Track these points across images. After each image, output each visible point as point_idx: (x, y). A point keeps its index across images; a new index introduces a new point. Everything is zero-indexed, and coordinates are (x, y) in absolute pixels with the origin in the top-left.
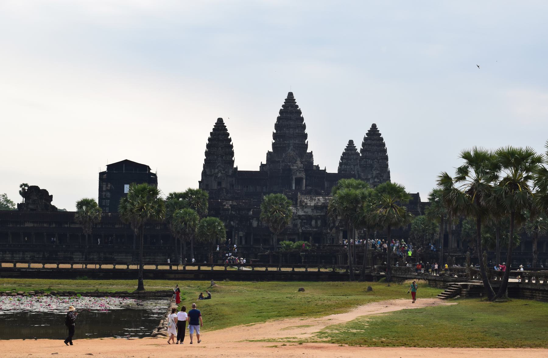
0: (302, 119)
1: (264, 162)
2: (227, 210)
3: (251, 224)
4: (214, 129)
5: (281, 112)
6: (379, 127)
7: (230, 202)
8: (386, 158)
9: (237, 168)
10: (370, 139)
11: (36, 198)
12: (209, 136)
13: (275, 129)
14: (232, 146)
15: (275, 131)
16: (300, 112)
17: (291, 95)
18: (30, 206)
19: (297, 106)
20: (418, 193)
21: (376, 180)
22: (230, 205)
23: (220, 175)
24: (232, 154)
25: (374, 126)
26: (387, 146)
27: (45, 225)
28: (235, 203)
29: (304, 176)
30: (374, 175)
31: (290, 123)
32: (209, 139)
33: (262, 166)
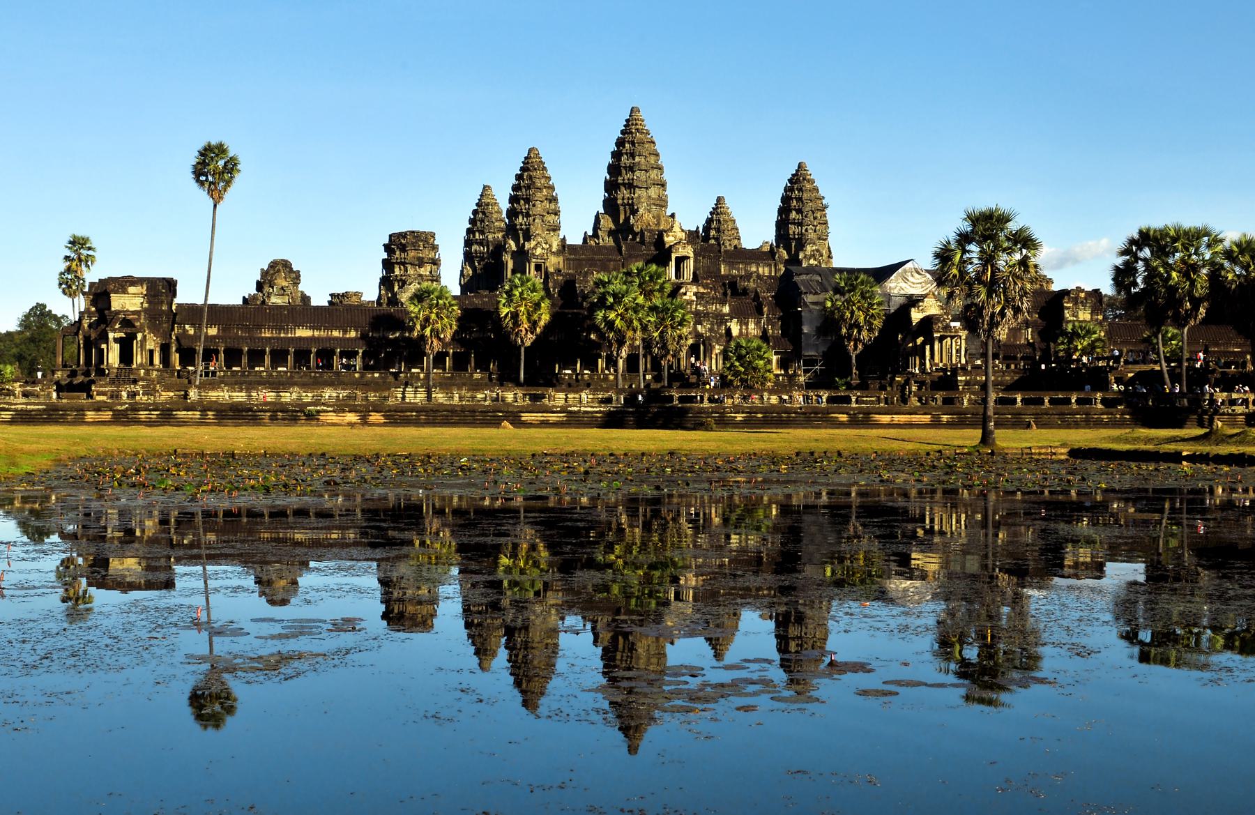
1: (590, 233)
2: (690, 302)
3: (729, 331)
4: (522, 169)
5: (620, 143)
7: (694, 289)
8: (826, 223)
9: (564, 240)
10: (800, 190)
11: (284, 284)
12: (514, 181)
13: (609, 173)
14: (554, 200)
18: (276, 300)
21: (812, 262)
22: (695, 294)
23: (539, 251)
24: (556, 213)
25: (801, 166)
27: (336, 333)
28: (702, 290)
29: (691, 255)
30: (808, 253)
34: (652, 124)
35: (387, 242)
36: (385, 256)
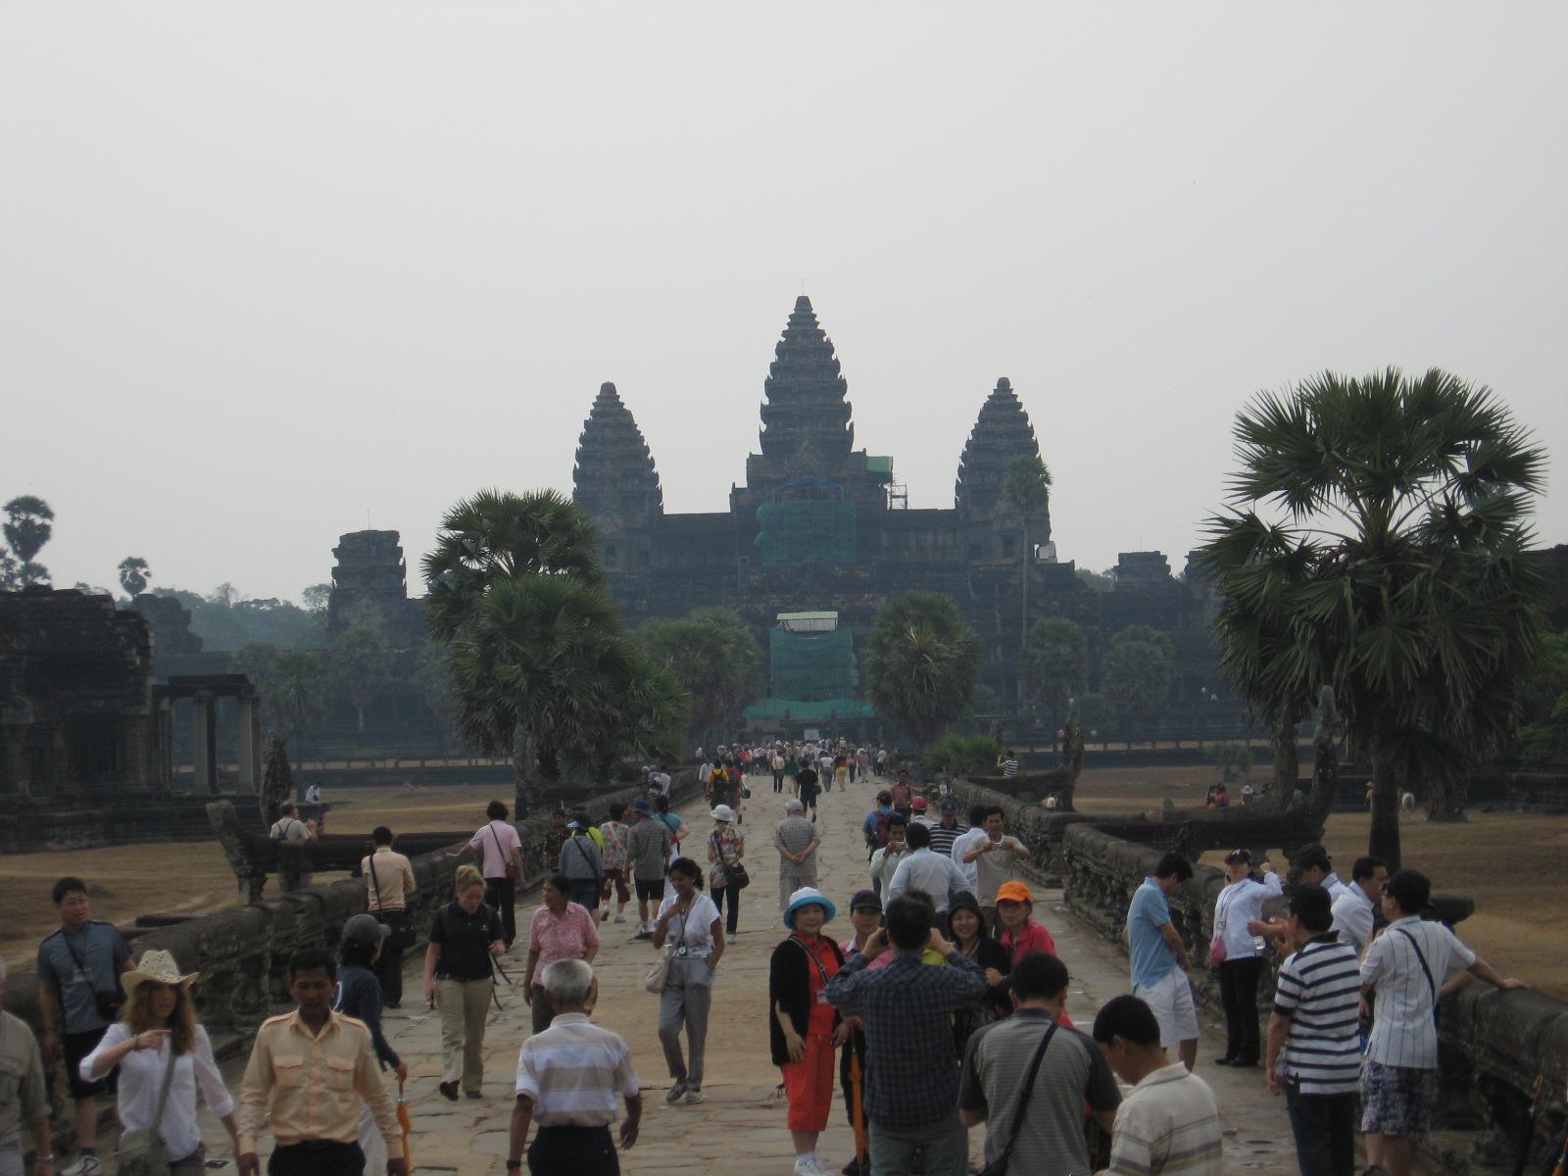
0: (836, 366)
1: (743, 483)
4: (592, 413)
5: (781, 350)
6: (1016, 388)
15: (766, 401)
16: (829, 348)
17: (803, 303)
19: (822, 333)
20: (1073, 561)
21: (1009, 524)
25: (1004, 384)
26: (1038, 435)
31: (805, 378)
32: (583, 439)
33: (736, 493)
34: (828, 321)
35: (336, 544)
36: (336, 563)
